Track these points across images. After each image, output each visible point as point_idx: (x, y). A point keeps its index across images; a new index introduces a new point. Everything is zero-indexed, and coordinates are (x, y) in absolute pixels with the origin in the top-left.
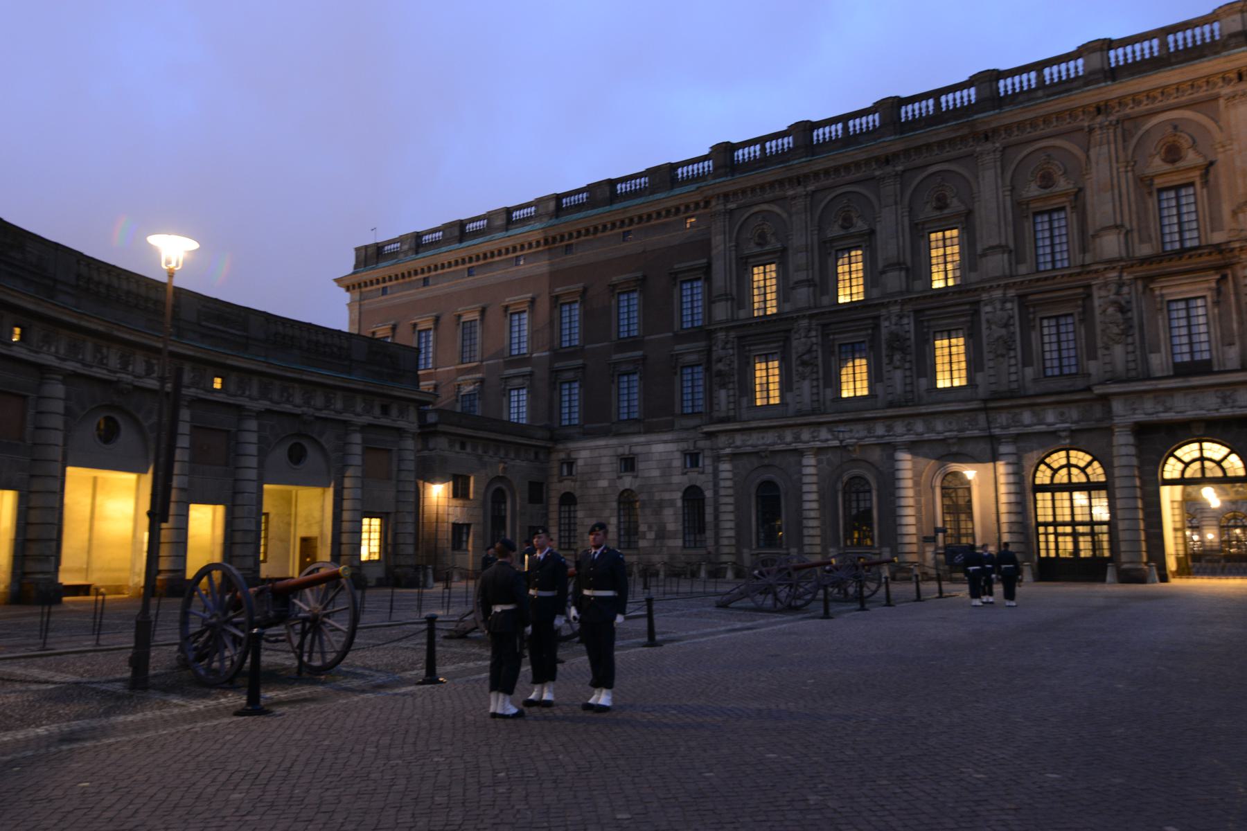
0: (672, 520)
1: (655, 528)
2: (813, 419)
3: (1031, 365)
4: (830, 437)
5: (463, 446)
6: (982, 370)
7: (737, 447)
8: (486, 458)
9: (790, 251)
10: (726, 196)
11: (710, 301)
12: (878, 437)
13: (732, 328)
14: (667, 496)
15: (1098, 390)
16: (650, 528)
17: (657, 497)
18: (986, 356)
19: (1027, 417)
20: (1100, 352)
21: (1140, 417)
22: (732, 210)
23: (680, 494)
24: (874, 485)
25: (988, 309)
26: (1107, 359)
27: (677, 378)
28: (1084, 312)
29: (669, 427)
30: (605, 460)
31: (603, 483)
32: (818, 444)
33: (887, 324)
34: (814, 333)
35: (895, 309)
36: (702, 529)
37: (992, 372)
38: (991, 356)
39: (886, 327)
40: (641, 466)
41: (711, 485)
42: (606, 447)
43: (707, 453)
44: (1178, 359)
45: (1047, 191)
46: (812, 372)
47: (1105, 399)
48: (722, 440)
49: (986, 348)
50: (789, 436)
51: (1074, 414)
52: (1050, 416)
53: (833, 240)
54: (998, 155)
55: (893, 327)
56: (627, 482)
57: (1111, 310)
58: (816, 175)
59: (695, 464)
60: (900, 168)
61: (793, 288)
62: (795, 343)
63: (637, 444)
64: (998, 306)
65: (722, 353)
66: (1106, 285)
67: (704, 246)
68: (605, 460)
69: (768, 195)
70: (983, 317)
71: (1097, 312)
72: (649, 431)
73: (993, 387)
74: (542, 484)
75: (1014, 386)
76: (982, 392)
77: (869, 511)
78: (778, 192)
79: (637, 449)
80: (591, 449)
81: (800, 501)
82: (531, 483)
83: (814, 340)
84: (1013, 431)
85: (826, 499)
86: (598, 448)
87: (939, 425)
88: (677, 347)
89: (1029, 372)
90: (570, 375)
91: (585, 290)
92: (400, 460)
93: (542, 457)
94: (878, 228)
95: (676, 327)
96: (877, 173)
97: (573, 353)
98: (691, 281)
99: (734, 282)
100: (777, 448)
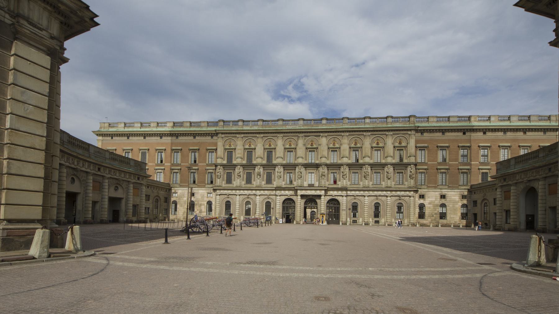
5: (148, 187)
18: (276, 179)
19: (283, 192)
21: (302, 194)
24: (252, 203)
27: (207, 175)
29: (204, 187)
35: (259, 166)
40: (195, 195)
47: (297, 190)
48: (218, 191)
50: (234, 191)
51: (291, 192)
52: (287, 192)
53: (247, 149)
76: (275, 186)
85: (241, 205)
87: (266, 192)
89: (284, 183)
90: (177, 171)
92: (141, 191)
94: (257, 148)
95: (207, 163)
97: (178, 165)
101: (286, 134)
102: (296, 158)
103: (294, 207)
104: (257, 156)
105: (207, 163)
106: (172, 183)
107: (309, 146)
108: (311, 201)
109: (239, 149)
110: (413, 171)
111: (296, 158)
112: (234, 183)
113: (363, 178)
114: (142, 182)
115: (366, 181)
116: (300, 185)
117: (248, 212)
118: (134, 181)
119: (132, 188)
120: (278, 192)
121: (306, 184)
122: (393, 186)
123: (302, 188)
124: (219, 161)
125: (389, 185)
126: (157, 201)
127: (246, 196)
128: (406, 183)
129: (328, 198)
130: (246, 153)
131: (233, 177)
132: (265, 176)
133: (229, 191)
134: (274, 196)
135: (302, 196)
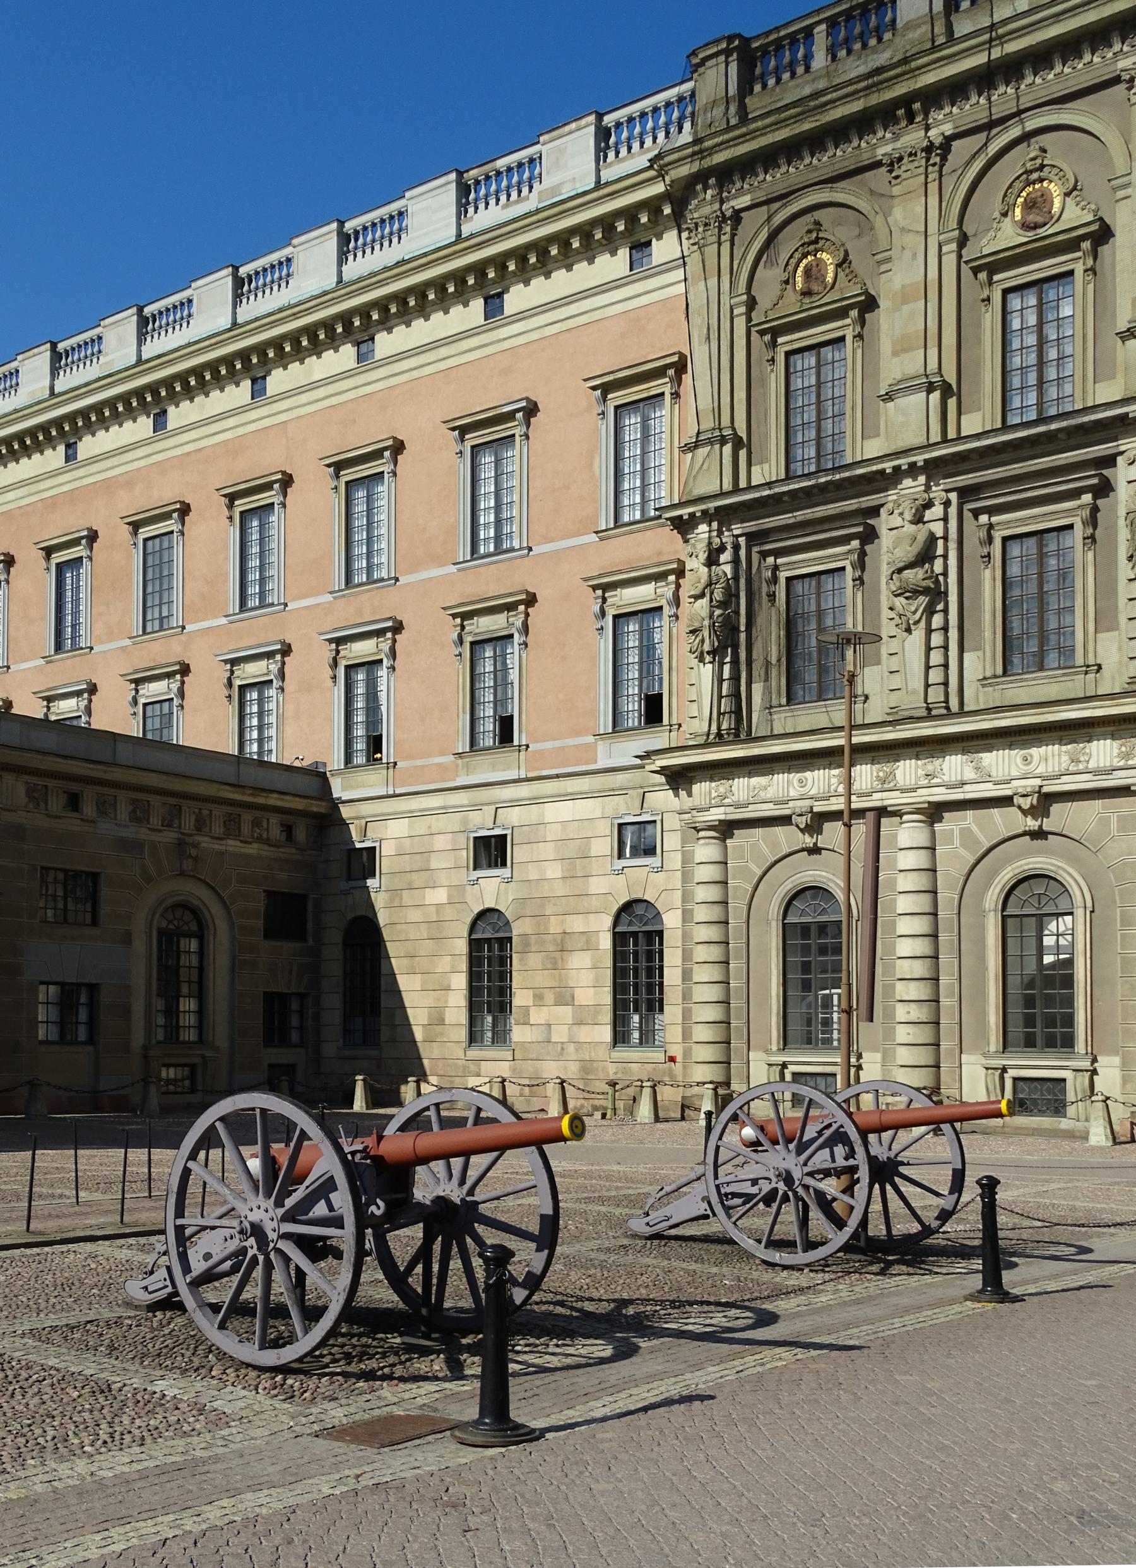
7: (737, 806)
12: (1096, 772)
14: (576, 924)
17: (555, 926)
22: (737, 217)
23: (608, 921)
30: (441, 842)
31: (439, 896)
32: (941, 795)
36: (655, 1005)
40: (517, 853)
42: (445, 810)
46: (930, 611)
56: (491, 889)
61: (888, 397)
62: (886, 539)
63: (515, 803)
68: (441, 842)
74: (303, 898)
79: (513, 817)
80: (411, 815)
83: (938, 529)
86: (424, 813)
93: (301, 834)
94: (1121, 220)
99: (741, 395)
106: (335, 760)
112: (871, 680)
127: (1005, 821)
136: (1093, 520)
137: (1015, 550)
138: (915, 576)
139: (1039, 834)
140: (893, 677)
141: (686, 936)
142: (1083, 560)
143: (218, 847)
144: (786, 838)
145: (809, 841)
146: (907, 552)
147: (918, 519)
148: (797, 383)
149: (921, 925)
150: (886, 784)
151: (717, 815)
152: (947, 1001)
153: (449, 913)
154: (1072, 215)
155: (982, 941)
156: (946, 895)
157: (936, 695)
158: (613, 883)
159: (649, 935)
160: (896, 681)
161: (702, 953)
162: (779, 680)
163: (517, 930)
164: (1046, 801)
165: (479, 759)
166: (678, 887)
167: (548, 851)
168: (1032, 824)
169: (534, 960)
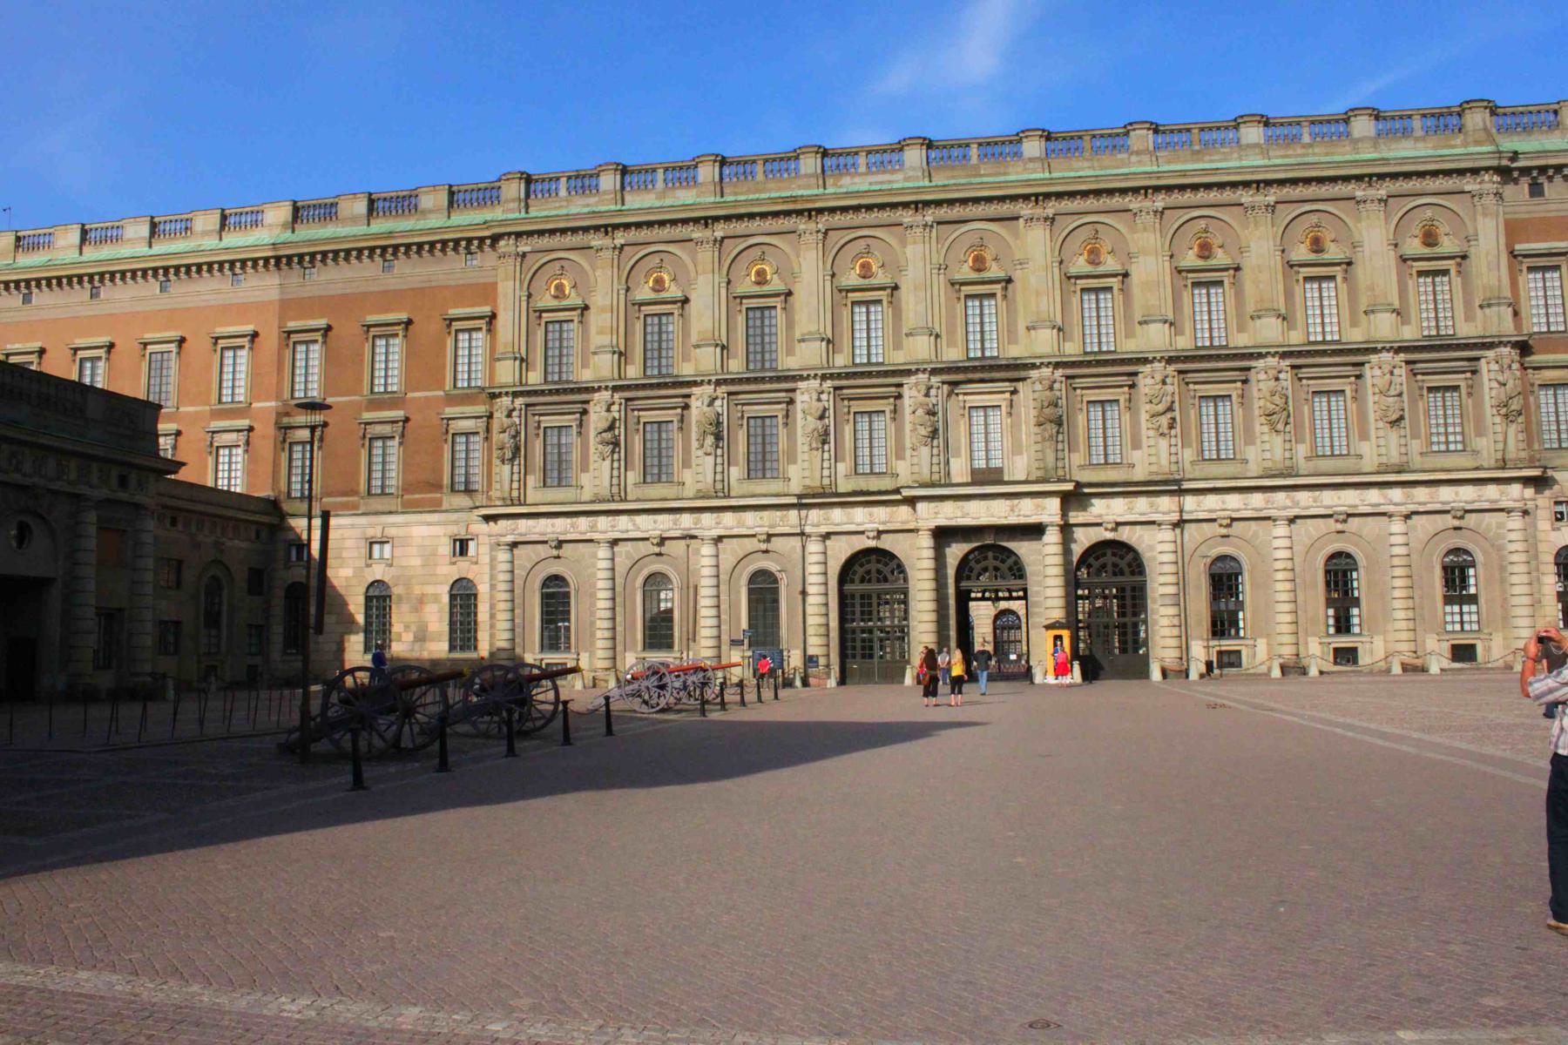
0: (437, 619)
1: (414, 628)
2: (614, 506)
3: (843, 460)
4: (630, 527)
5: (174, 522)
6: (795, 462)
8: (200, 538)
9: (592, 310)
10: (519, 235)
11: (494, 359)
13: (522, 394)
14: (430, 590)
15: (906, 493)
16: (407, 627)
17: (417, 590)
18: (800, 449)
19: (837, 514)
20: (908, 453)
21: (943, 522)
22: (524, 255)
23: (447, 588)
25: (806, 397)
26: (915, 460)
28: (895, 411)
29: (435, 508)
30: (349, 543)
33: (699, 403)
34: (615, 408)
37: (806, 465)
38: (806, 448)
39: (698, 407)
41: (487, 578)
43: (487, 540)
44: (976, 464)
45: (866, 282)
46: (613, 452)
49: (800, 439)
50: (583, 522)
51: (881, 513)
52: (860, 517)
54: (820, 236)
55: (706, 409)
57: (920, 412)
58: (627, 226)
59: (463, 551)
60: (719, 234)
63: (393, 525)
64: (815, 396)
65: (507, 421)
66: (917, 384)
67: (487, 292)
68: (349, 543)
69: (569, 240)
70: (799, 406)
71: (908, 411)
72: (410, 508)
73: (808, 482)
75: (826, 481)
76: (796, 486)
77: (670, 611)
78: (578, 239)
81: (593, 595)
82: (250, 569)
84: (824, 529)
87: (749, 517)
88: (448, 410)
91: (329, 328)
93: (264, 534)
94: (693, 297)
96: (694, 236)
98: (470, 331)
99: (524, 338)
100: (569, 537)
101: (838, 219)
102: (898, 337)
103: (905, 592)
104: (694, 339)
105: (448, 385)
107: (966, 272)
108: (988, 558)
109: (602, 310)
110: (1513, 377)
111: (898, 337)
112: (585, 479)
113: (1260, 427)
114: (140, 498)
115: (1278, 440)
116: (926, 476)
117: (659, 631)
118: (102, 493)
119: (92, 530)
120: (816, 520)
121: (959, 470)
122: (1417, 461)
123: (937, 489)
124: (506, 373)
125: (1394, 457)
126: (214, 589)
128: (1482, 443)
129: (1084, 539)
130: (639, 326)
131: (575, 456)
132: (742, 436)
133: (560, 527)
134: (796, 542)
135: (943, 535)
136: (682, 421)
137: (648, 427)
138: (608, 436)
139: (660, 554)
140: (596, 477)
141: (492, 597)
142: (678, 437)
143: (229, 544)
144: (543, 551)
145: (555, 552)
146: (605, 425)
147: (608, 410)
148: (550, 336)
149: (608, 594)
150: (593, 528)
151: (510, 539)
152: (619, 629)
153: (354, 582)
154: (673, 292)
155: (634, 602)
156: (619, 581)
157: (615, 489)
158: (450, 571)
159: (469, 596)
160: (597, 482)
161: (502, 606)
162: (539, 475)
163: (396, 591)
164: (663, 541)
165: (372, 500)
166: (487, 570)
167: (413, 551)
168: (657, 550)
169: (405, 607)
